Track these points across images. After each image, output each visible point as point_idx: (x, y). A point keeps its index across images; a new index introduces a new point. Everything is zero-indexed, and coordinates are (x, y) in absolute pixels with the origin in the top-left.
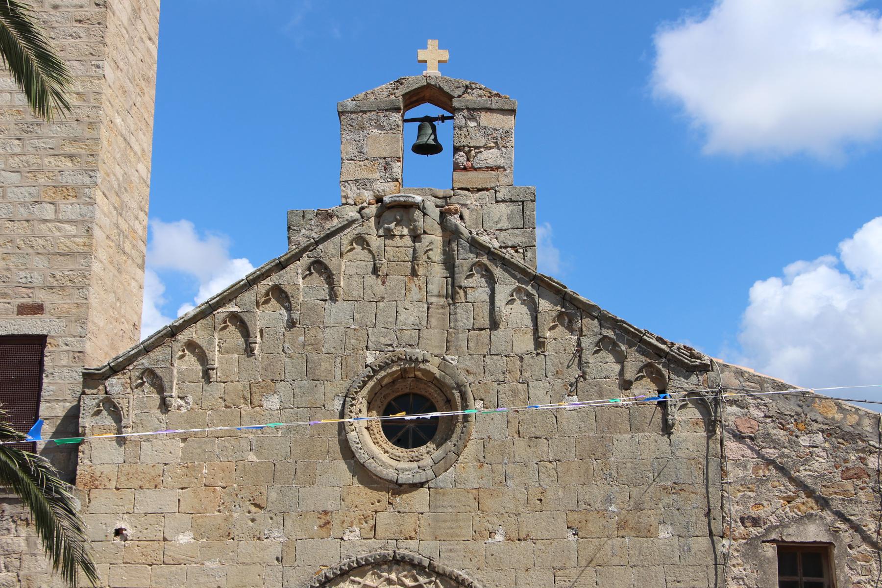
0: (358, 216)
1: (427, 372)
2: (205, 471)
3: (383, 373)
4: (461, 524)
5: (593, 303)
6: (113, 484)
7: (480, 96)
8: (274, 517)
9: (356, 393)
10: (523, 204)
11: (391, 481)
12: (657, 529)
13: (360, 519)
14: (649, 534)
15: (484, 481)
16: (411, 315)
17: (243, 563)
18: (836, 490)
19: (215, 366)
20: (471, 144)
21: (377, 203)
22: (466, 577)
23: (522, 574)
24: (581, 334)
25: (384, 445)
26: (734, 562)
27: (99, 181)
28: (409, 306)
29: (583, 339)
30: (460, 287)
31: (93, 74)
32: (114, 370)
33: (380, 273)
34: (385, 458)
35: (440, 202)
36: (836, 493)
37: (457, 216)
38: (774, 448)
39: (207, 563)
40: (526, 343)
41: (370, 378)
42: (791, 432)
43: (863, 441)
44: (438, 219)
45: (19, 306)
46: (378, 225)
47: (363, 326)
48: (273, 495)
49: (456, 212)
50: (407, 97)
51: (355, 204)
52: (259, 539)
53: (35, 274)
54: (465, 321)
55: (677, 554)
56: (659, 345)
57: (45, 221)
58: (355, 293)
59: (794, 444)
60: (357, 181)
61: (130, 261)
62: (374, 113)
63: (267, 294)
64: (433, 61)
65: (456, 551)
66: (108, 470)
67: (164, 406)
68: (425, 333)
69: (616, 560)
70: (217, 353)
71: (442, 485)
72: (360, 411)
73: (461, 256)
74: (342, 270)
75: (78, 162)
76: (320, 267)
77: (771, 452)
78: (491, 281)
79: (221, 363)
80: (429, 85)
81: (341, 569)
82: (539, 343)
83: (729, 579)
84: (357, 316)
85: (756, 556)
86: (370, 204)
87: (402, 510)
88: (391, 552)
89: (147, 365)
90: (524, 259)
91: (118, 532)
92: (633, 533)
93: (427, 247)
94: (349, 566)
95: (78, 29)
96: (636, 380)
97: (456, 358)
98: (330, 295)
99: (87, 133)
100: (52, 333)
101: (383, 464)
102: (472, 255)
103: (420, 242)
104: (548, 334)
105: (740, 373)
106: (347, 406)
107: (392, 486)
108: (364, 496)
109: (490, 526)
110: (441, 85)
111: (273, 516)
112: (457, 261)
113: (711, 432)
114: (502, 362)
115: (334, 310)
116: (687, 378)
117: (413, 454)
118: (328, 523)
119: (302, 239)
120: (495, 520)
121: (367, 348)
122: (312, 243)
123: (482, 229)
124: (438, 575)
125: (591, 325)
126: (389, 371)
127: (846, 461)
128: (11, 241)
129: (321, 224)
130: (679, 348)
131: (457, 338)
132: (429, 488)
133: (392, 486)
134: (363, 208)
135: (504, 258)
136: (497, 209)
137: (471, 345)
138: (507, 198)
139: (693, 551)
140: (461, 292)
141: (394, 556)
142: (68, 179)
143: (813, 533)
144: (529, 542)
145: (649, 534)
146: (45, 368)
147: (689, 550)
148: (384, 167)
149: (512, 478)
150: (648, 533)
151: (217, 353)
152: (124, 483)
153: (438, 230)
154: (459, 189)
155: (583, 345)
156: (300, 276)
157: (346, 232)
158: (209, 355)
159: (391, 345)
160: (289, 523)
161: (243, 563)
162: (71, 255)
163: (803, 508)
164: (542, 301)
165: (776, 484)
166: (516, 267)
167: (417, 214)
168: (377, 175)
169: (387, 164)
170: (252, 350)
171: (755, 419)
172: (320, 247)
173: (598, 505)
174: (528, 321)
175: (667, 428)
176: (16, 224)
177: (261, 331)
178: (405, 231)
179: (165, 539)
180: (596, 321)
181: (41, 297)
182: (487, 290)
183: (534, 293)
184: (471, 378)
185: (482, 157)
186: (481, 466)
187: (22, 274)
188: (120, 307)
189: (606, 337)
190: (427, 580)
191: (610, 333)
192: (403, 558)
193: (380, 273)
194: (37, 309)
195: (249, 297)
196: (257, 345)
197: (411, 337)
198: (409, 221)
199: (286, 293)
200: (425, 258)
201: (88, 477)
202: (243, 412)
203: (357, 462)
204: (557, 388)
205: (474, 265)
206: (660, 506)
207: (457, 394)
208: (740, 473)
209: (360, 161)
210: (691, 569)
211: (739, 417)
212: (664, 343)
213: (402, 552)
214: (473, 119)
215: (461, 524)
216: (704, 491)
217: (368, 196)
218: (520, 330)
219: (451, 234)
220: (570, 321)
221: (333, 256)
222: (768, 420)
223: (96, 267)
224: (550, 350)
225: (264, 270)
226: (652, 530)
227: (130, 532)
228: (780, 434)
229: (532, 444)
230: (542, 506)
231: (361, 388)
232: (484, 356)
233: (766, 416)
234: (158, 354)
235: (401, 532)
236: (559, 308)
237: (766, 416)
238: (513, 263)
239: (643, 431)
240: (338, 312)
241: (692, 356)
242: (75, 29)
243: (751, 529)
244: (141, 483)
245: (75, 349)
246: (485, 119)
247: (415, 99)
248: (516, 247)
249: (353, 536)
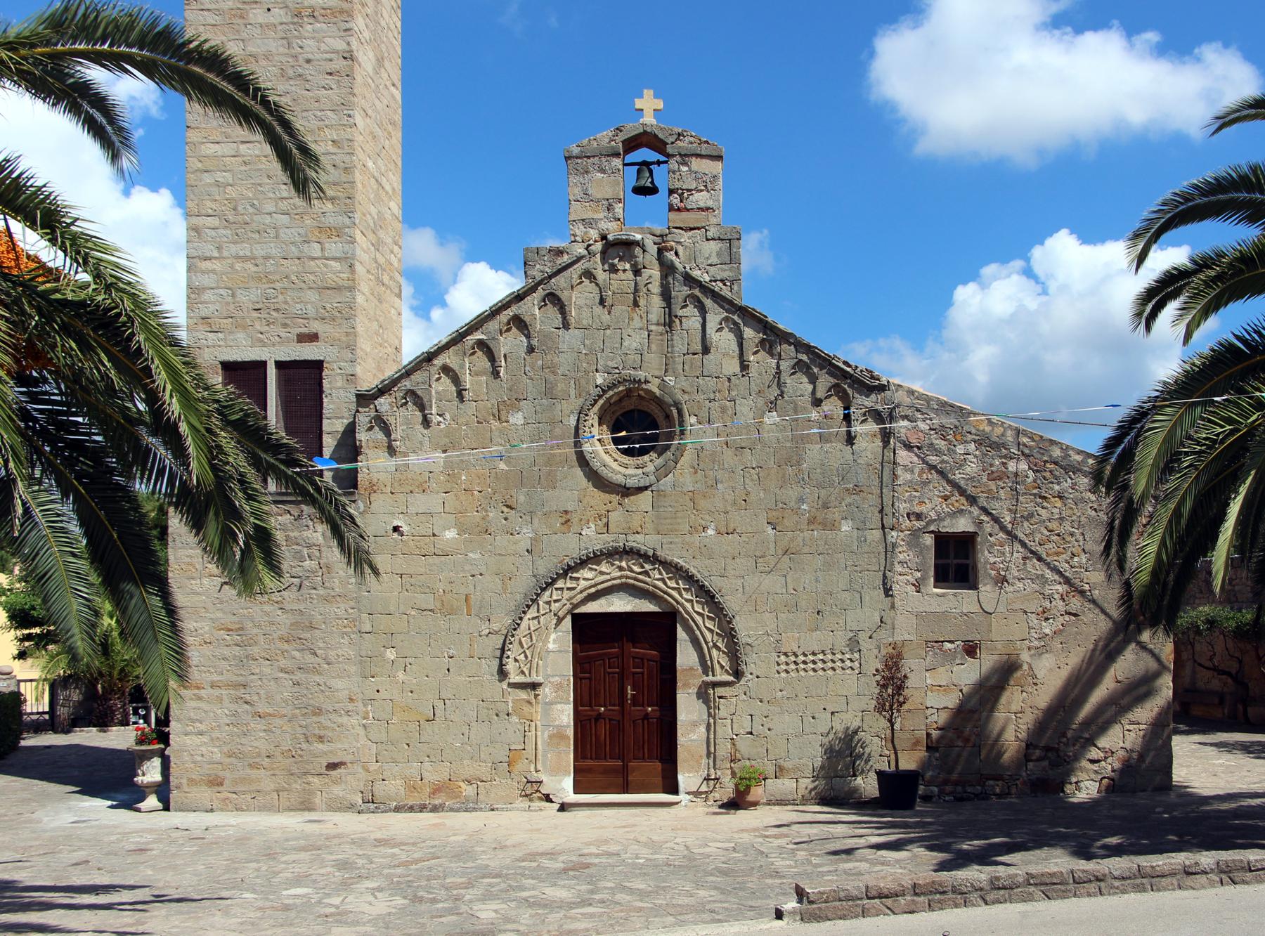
0: (585, 252)
1: (648, 392)
2: (464, 478)
3: (611, 393)
4: (680, 521)
5: (790, 331)
6: (388, 489)
7: (691, 143)
8: (524, 516)
9: (589, 410)
11: (620, 486)
12: (840, 523)
13: (595, 518)
14: (833, 528)
15: (698, 485)
16: (635, 341)
17: (500, 555)
18: (983, 490)
19: (467, 387)
20: (684, 187)
21: (602, 240)
22: (684, 564)
23: (729, 561)
24: (780, 359)
25: (614, 455)
26: (900, 549)
27: (357, 221)
28: (632, 333)
29: (782, 363)
30: (676, 316)
31: (345, 123)
32: (382, 391)
33: (606, 304)
34: (614, 465)
35: (657, 240)
36: (982, 492)
37: (672, 253)
38: (936, 455)
39: (471, 555)
40: (733, 366)
41: (600, 397)
42: (950, 443)
43: (1006, 449)
44: (656, 256)
45: (298, 335)
46: (604, 261)
47: (592, 351)
48: (522, 498)
49: (672, 250)
51: (583, 242)
52: (512, 534)
53: (309, 306)
54: (681, 347)
55: (856, 543)
56: (845, 368)
57: (314, 259)
58: (585, 322)
59: (952, 452)
60: (583, 220)
61: (388, 291)
62: (597, 158)
63: (508, 323)
65: (675, 543)
66: (384, 477)
67: (426, 423)
68: (647, 357)
69: (806, 550)
70: (468, 375)
71: (663, 488)
72: (592, 425)
73: (676, 289)
75: (338, 204)
76: (553, 299)
77: (933, 459)
78: (703, 311)
79: (472, 384)
80: (645, 132)
81: (580, 559)
82: (744, 367)
83: (896, 563)
84: (587, 342)
85: (918, 545)
86: (596, 241)
87: (630, 509)
88: (621, 544)
89: (409, 387)
91: (396, 529)
92: (820, 527)
94: (587, 556)
95: (330, 81)
96: (826, 398)
97: (673, 379)
98: (563, 324)
99: (344, 178)
100: (328, 359)
101: (613, 471)
102: (685, 288)
103: (641, 276)
104: (752, 358)
105: (911, 392)
106: (581, 421)
107: (621, 489)
108: (598, 498)
109: (703, 522)
110: (656, 132)
111: (522, 515)
113: (886, 442)
114: (712, 382)
115: (567, 337)
116: (867, 396)
117: (638, 462)
118: (569, 520)
119: (536, 273)
120: (707, 517)
121: (597, 371)
124: (661, 563)
125: (787, 350)
126: (616, 390)
127: (991, 465)
128: (286, 277)
130: (862, 371)
131: (674, 362)
132: (652, 491)
133: (621, 489)
134: (589, 245)
135: (714, 291)
137: (686, 367)
138: (716, 237)
139: (868, 541)
140: (677, 321)
141: (624, 548)
142: (330, 220)
143: (962, 525)
144: (736, 535)
145: (833, 528)
146: (324, 389)
147: (865, 540)
149: (722, 482)
150: (832, 526)
151: (468, 375)
152: (397, 489)
153: (657, 266)
155: (781, 368)
156: (536, 307)
157: (575, 266)
158: (462, 378)
159: (617, 368)
160: (536, 521)
161: (500, 555)
162: (338, 289)
163: (956, 504)
164: (746, 329)
165: (937, 485)
166: (724, 299)
167: (638, 250)
168: (601, 215)
169: (610, 205)
170: (498, 373)
171: (922, 431)
172: (553, 280)
173: (792, 504)
174: (735, 346)
175: (850, 439)
176: (290, 261)
177: (505, 356)
178: (628, 266)
179: (434, 535)
180: (792, 347)
181: (315, 327)
182: (700, 319)
183: (740, 321)
184: (686, 397)
186: (696, 473)
187: (298, 306)
188: (383, 333)
189: (801, 360)
190: (651, 567)
191: (804, 358)
192: (631, 549)
193: (606, 304)
194: (313, 337)
195: (493, 325)
197: (635, 361)
198: (630, 257)
199: (525, 322)
200: (645, 290)
201: (367, 483)
202: (493, 427)
203: (591, 469)
204: (759, 405)
205: (688, 296)
206: (843, 504)
207: (674, 411)
208: (909, 477)
210: (866, 555)
211: (909, 429)
212: (849, 366)
213: (630, 544)
214: (685, 164)
215: (680, 521)
216: (879, 491)
217: (594, 234)
218: (728, 354)
219: (667, 269)
220: (771, 347)
221: (565, 289)
222: (933, 432)
223: (360, 299)
224: (753, 371)
225: (504, 302)
226: (836, 524)
227: (405, 529)
228: (941, 444)
229: (738, 453)
230: (746, 505)
231: (593, 405)
232: (698, 378)
233: (931, 429)
234: (418, 377)
235: (630, 528)
236: (761, 335)
237: (931, 429)
239: (831, 442)
240: (570, 339)
241: (873, 377)
242: (327, 82)
243: (915, 522)
244: (411, 489)
245: (348, 372)
246: (696, 164)
249: (590, 531)
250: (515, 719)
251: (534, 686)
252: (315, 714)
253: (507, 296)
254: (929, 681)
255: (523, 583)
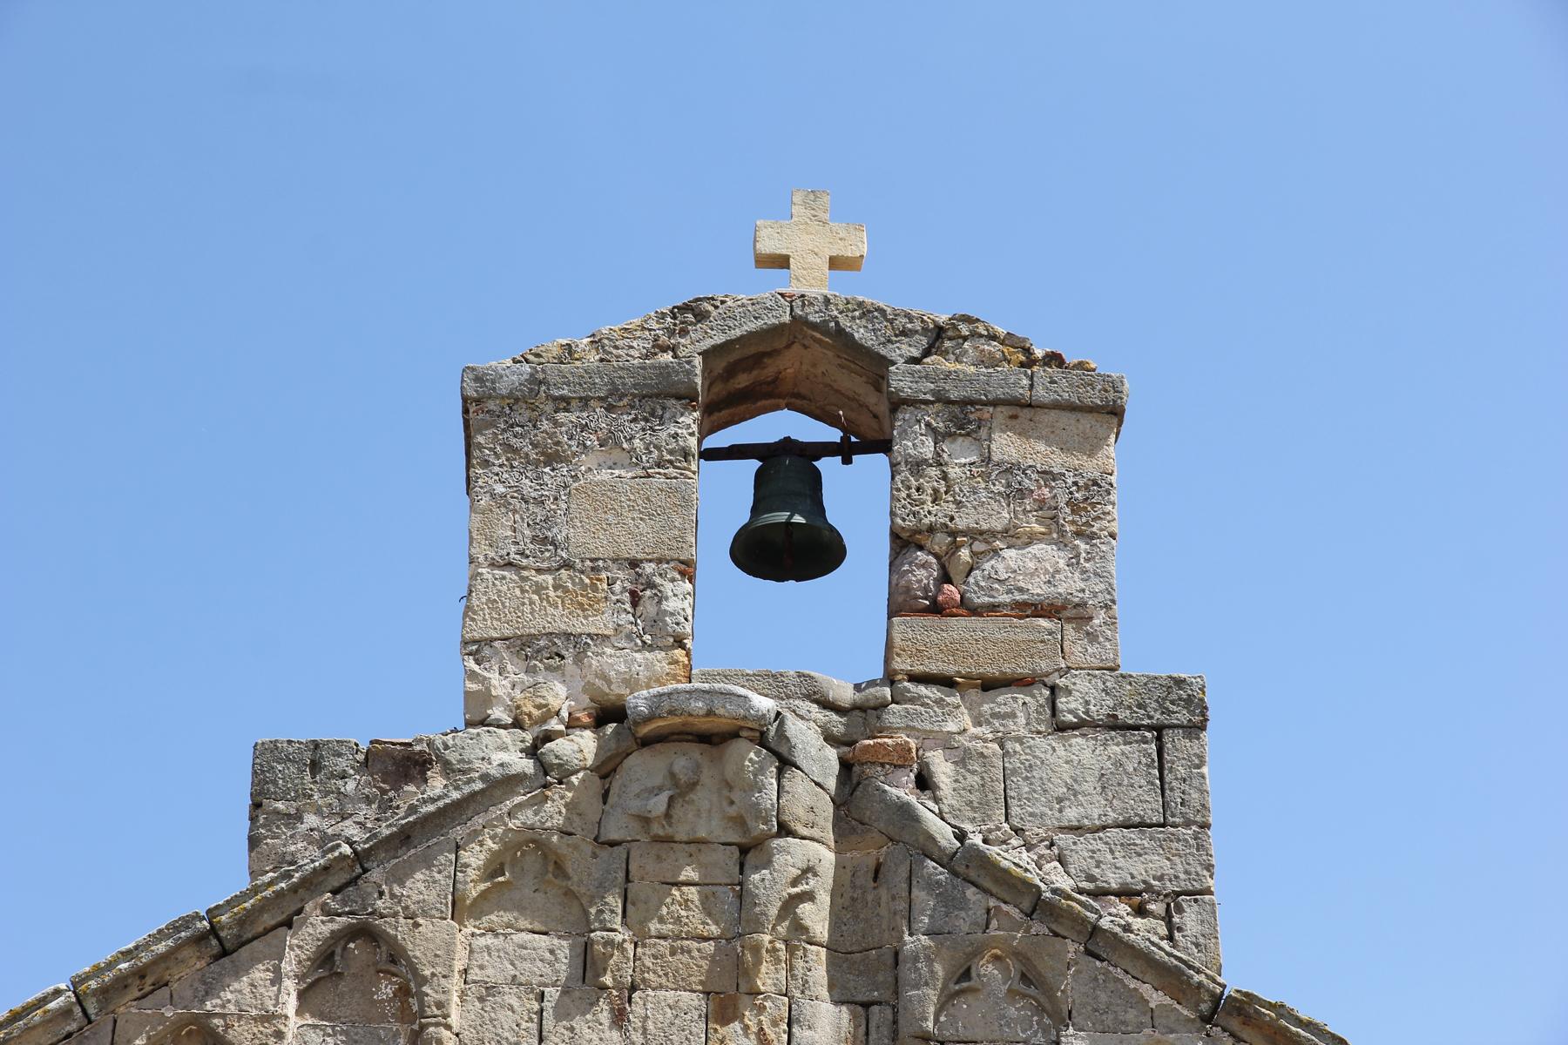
0: (527, 766)
10: (1159, 739)
20: (961, 523)
33: (607, 980)
35: (837, 723)
50: (720, 365)
51: (517, 724)
64: (811, 259)
74: (458, 966)
90: (1170, 938)
93: (794, 883)
103: (768, 863)
110: (845, 322)
112: (907, 938)
122: (343, 857)
123: (1006, 826)
129: (384, 792)
135: (1096, 929)
136: (1061, 752)
138: (1099, 711)
148: (633, 594)
154: (916, 678)
185: (1000, 567)
193: (607, 980)
209: (539, 571)
217: (559, 695)
225: (145, 957)
238: (1130, 947)
247: (742, 381)
248: (1139, 894)
253: (161, 935)
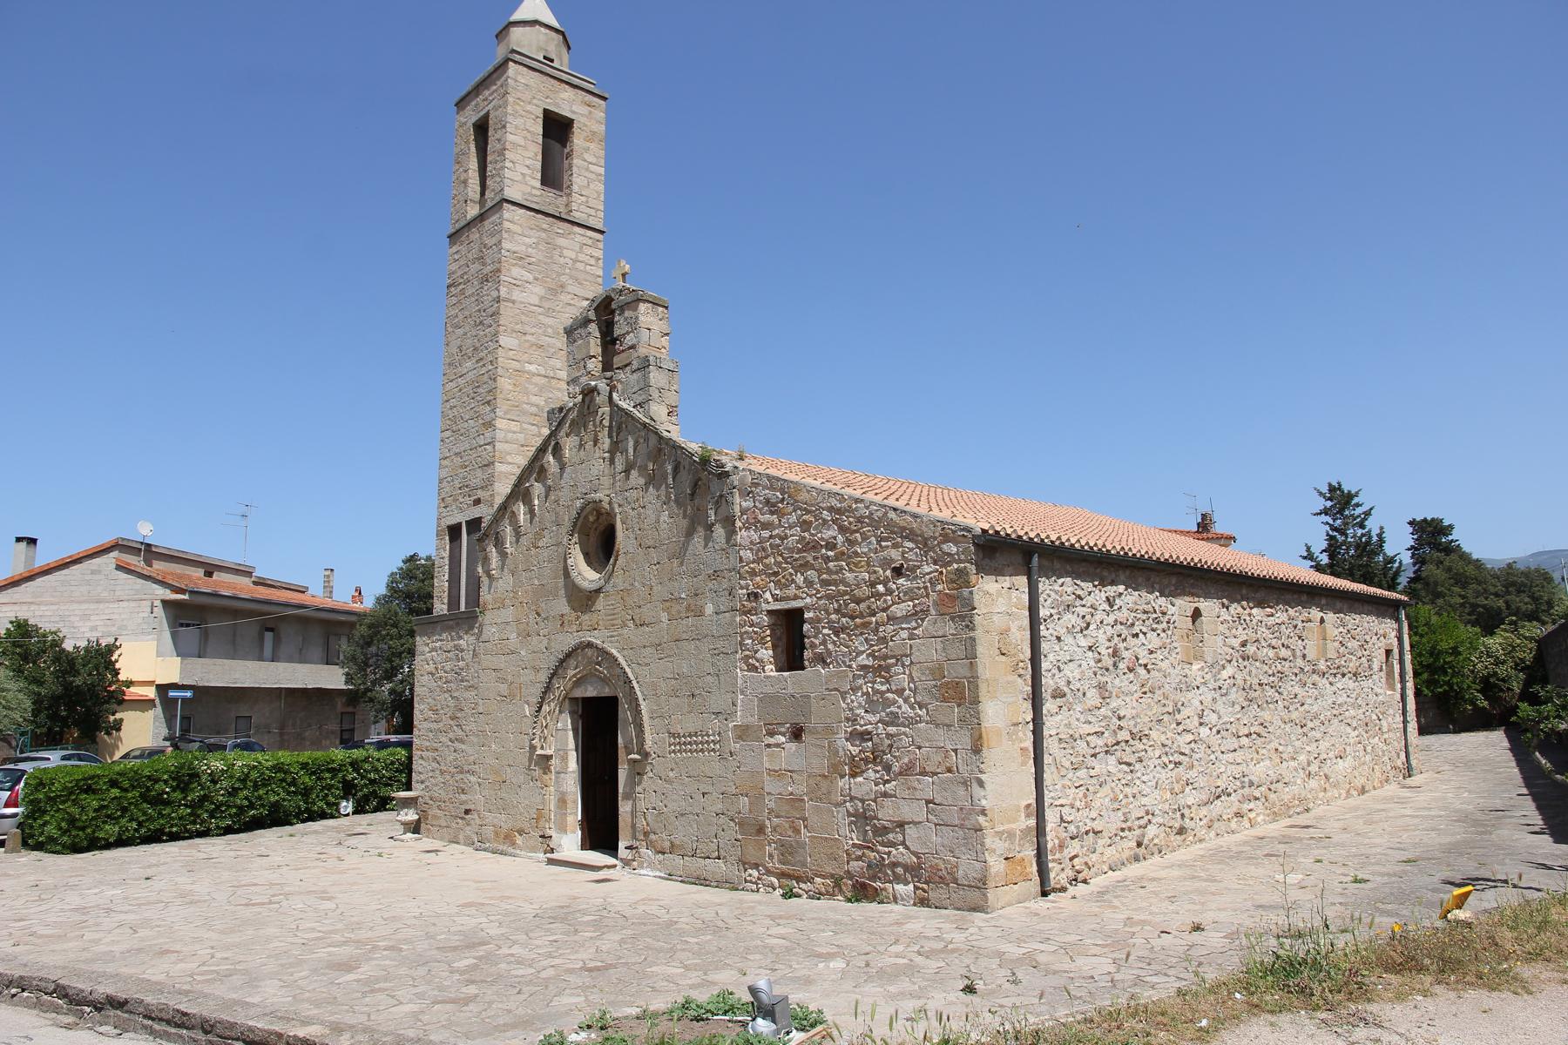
101: (584, 579)
150: (701, 614)
196: (536, 507)
250: (539, 783)
251: (549, 758)
252: (462, 773)
254: (767, 765)
255: (543, 677)
